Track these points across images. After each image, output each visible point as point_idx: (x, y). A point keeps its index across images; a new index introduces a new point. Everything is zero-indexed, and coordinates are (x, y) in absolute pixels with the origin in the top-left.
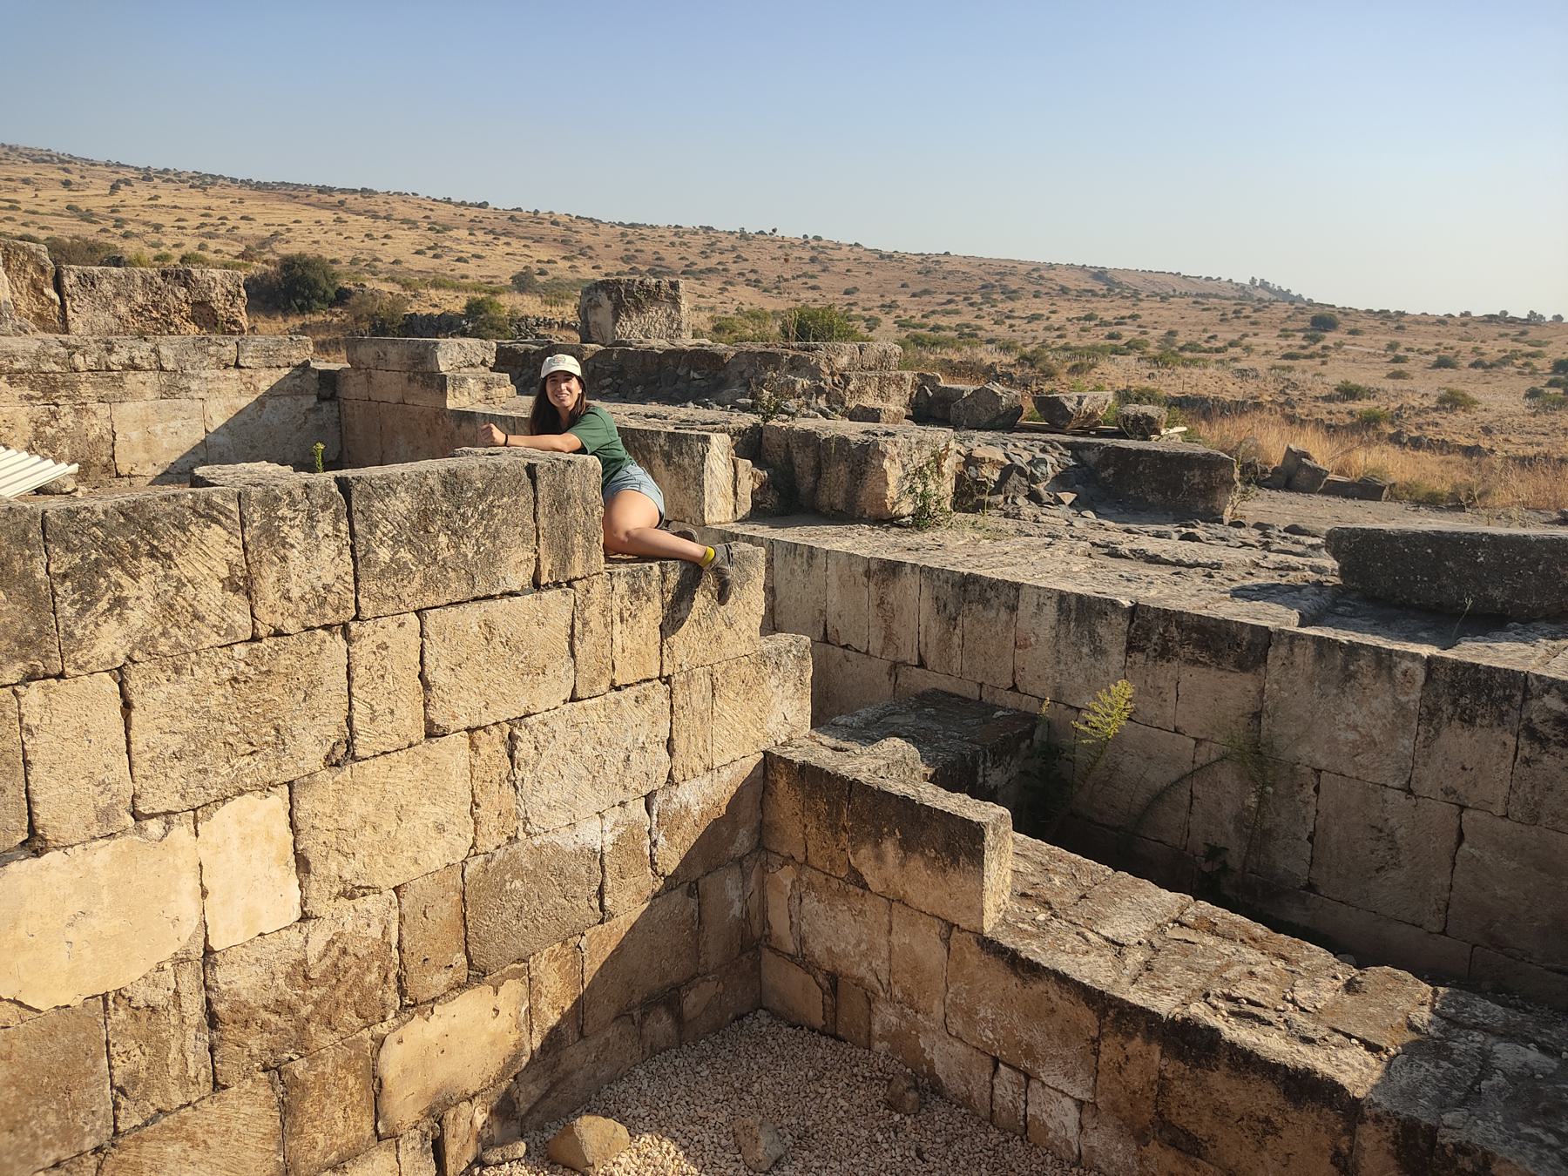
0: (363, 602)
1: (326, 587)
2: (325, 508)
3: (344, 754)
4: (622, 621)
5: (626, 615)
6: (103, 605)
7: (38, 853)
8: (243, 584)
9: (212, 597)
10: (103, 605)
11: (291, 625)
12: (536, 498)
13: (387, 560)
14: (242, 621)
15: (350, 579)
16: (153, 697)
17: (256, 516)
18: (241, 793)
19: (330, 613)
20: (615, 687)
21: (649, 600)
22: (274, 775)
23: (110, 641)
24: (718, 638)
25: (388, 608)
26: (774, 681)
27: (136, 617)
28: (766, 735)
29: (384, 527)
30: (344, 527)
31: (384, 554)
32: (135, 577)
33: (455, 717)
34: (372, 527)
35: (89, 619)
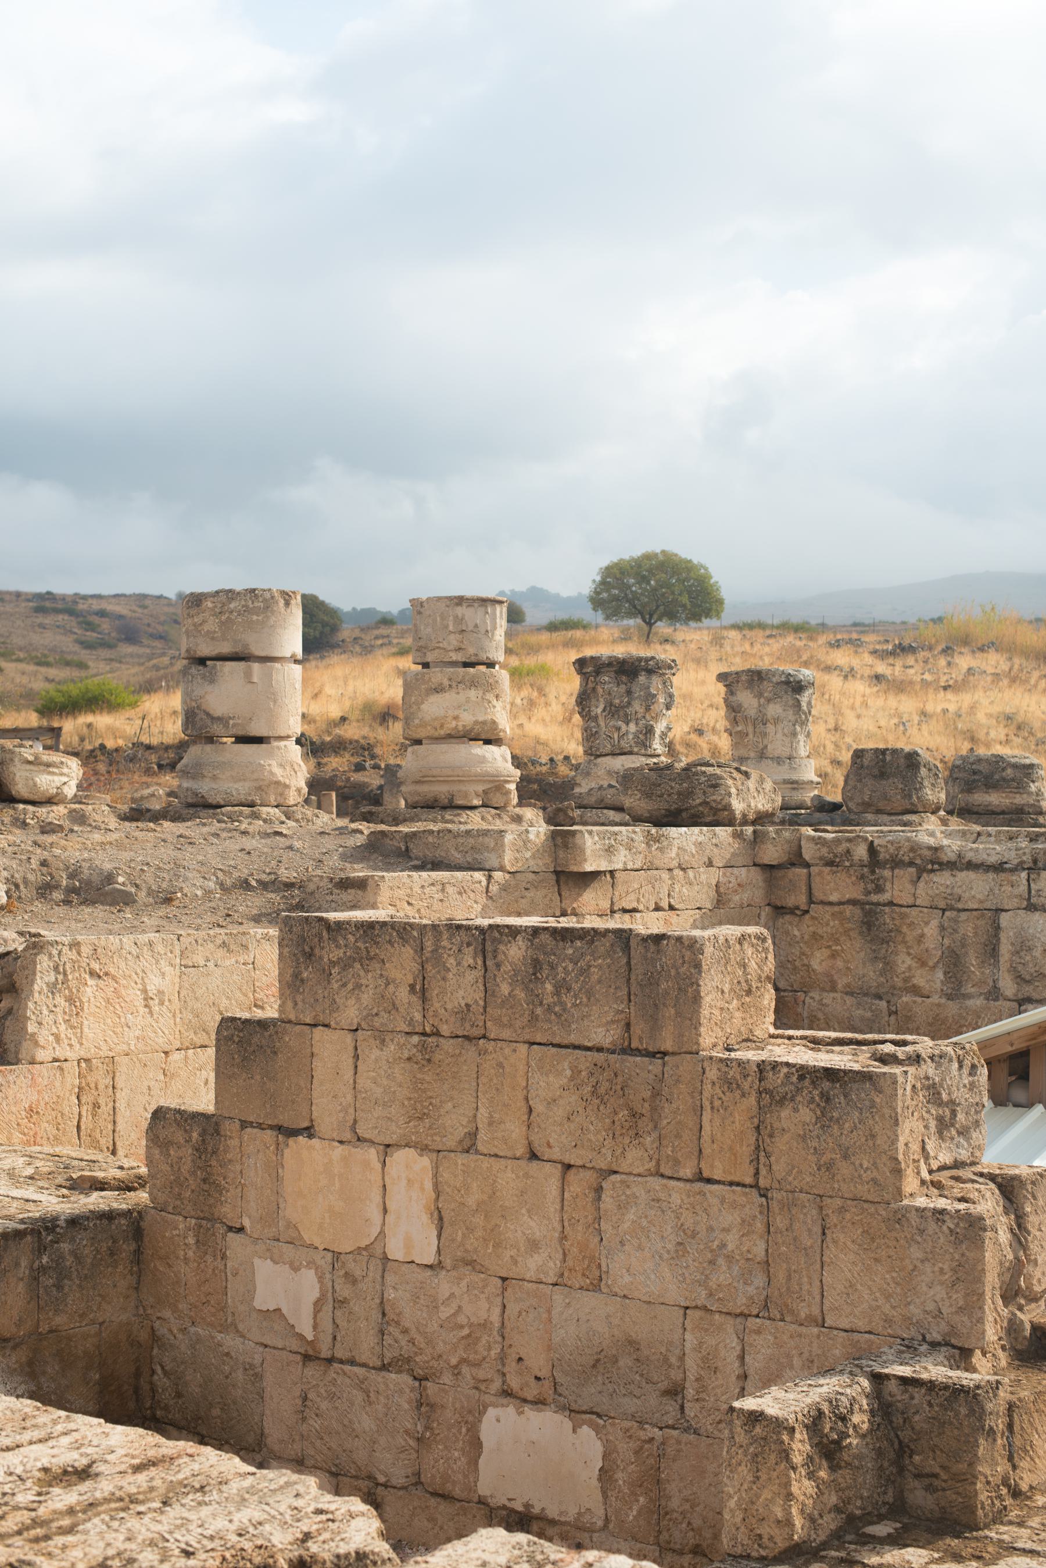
0: (489, 1024)
1: (467, 1005)
2: (469, 945)
3: (469, 1145)
4: (712, 1108)
5: (717, 1103)
6: (350, 986)
7: (311, 1136)
8: (421, 991)
9: (403, 995)
10: (350, 986)
11: (445, 1030)
12: (629, 963)
13: (506, 993)
14: (418, 1016)
15: (482, 1003)
16: (372, 1054)
17: (429, 944)
18: (407, 1145)
19: (467, 1026)
20: (700, 1178)
21: (743, 1095)
22: (428, 1141)
23: (350, 1013)
24: (829, 1166)
25: (506, 1034)
26: (916, 1253)
27: (366, 998)
28: (907, 1319)
29: (507, 967)
30: (480, 962)
31: (505, 989)
32: (367, 971)
33: (549, 1146)
34: (498, 966)
35: (343, 992)
